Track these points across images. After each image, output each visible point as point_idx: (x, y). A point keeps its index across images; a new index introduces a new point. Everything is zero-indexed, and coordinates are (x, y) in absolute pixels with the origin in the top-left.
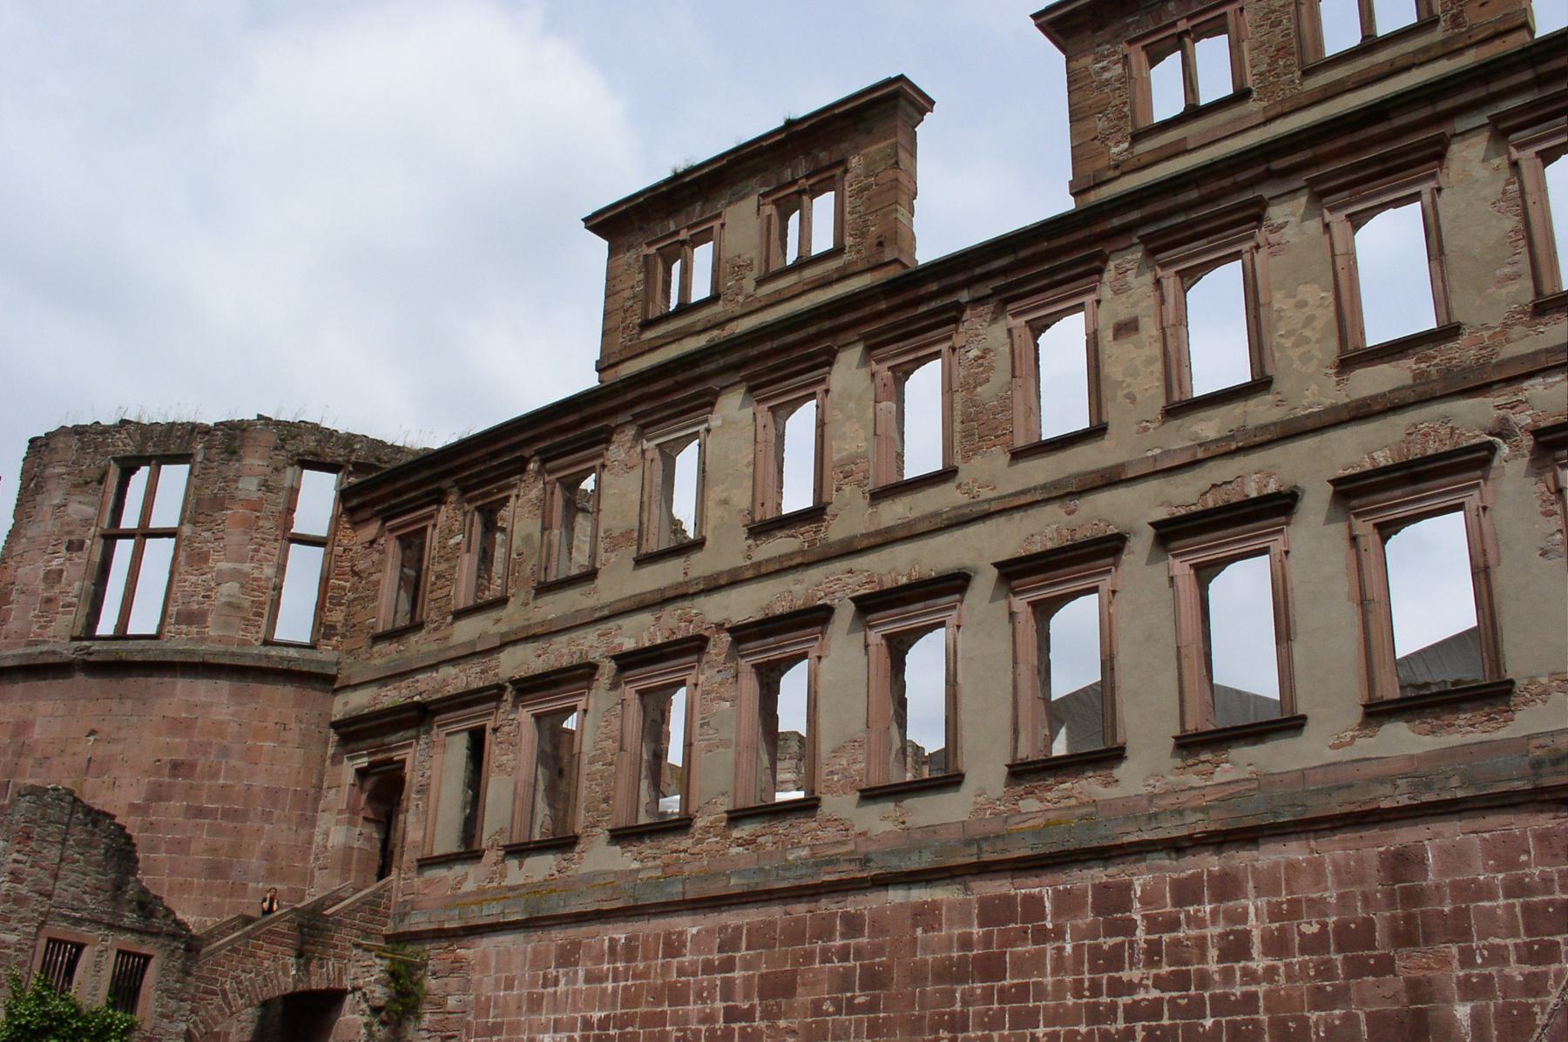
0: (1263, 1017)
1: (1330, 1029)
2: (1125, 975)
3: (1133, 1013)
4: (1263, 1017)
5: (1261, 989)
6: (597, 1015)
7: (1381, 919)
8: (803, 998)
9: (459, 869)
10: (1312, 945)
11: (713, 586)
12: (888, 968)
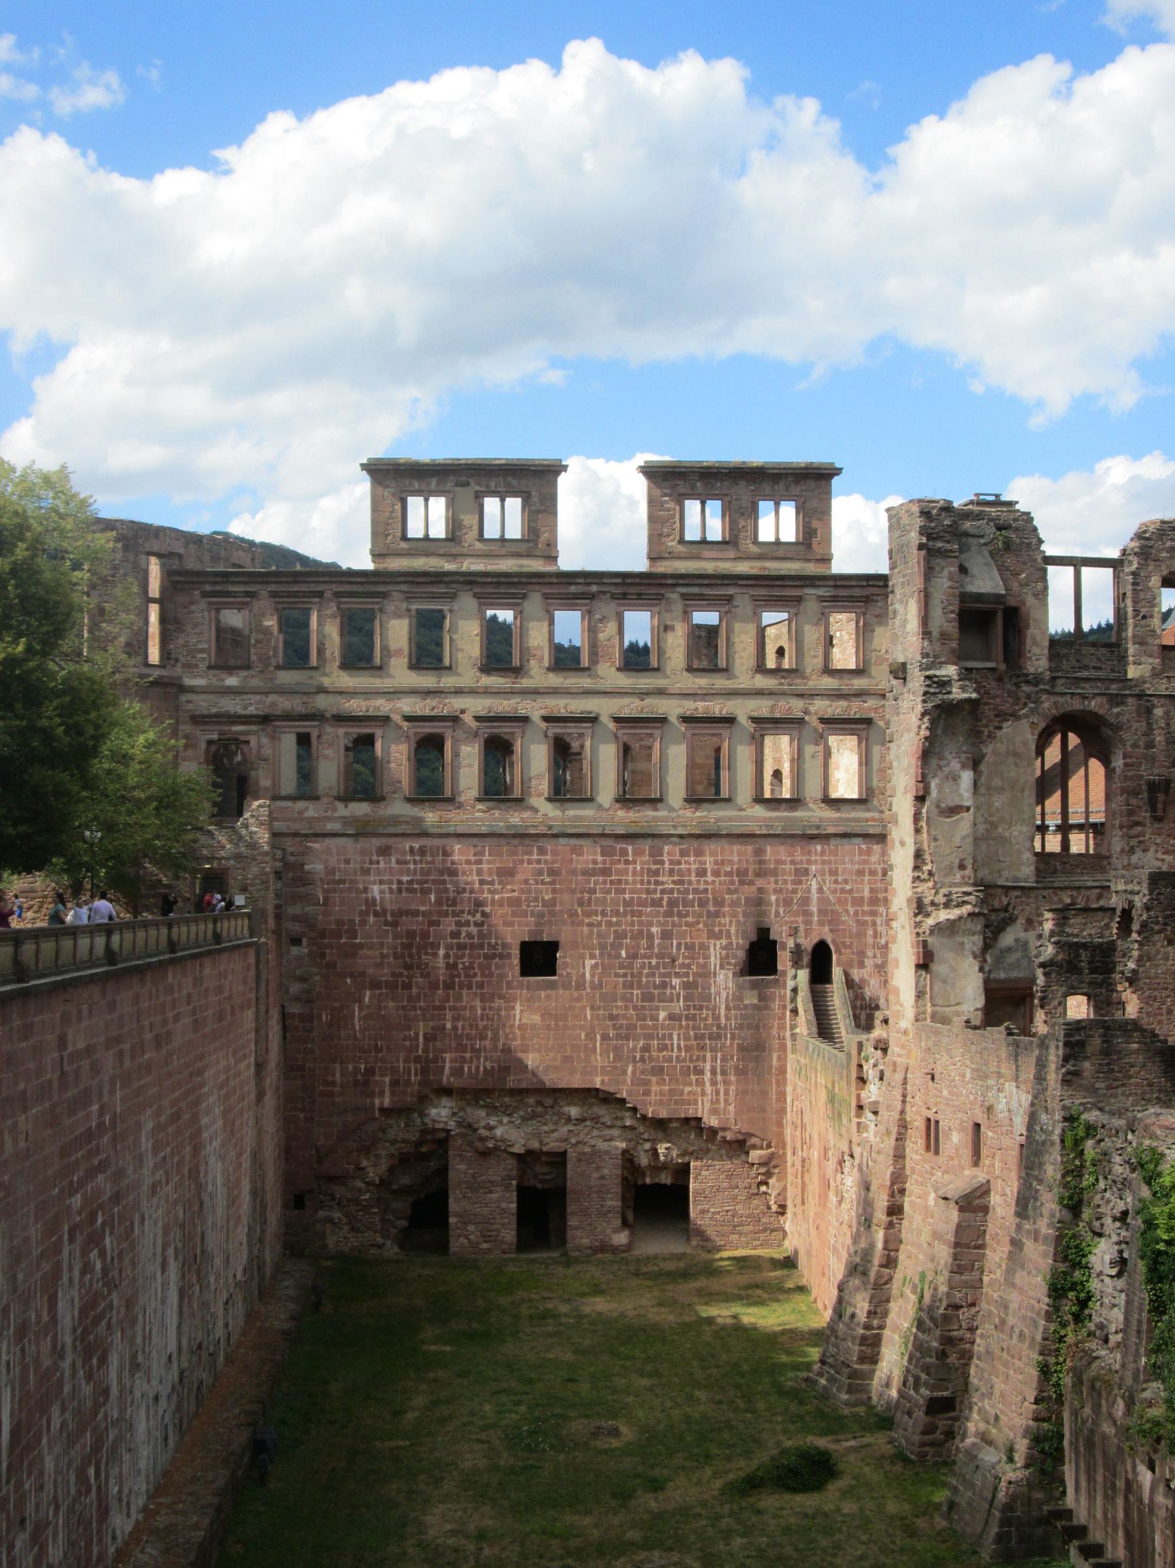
0: (710, 896)
1: (732, 901)
2: (660, 879)
3: (663, 892)
4: (710, 896)
5: (710, 887)
6: (405, 879)
7: (751, 867)
8: (519, 877)
9: (301, 804)
10: (727, 874)
11: (459, 692)
12: (560, 869)
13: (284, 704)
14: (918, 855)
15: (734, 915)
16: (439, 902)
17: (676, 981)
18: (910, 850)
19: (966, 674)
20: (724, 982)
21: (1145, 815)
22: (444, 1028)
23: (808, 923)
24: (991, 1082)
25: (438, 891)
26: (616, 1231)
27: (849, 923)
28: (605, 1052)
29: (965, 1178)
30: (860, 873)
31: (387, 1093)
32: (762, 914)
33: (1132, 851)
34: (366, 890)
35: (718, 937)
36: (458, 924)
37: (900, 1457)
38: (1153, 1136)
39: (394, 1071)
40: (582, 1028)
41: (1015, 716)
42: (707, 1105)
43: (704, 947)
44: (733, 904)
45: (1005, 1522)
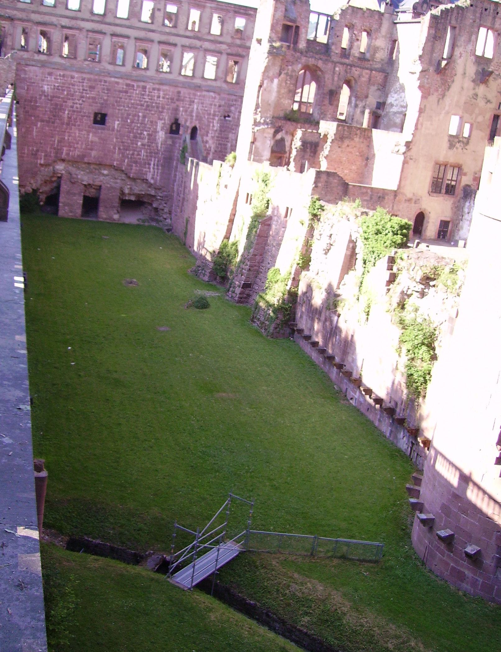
3: (145, 102)
6: (57, 85)
8: (96, 90)
10: (168, 99)
11: (83, 20)
13: (19, 15)
15: (168, 113)
16: (68, 94)
17: (145, 133)
20: (161, 135)
22: (64, 139)
23: (192, 119)
25: (68, 91)
26: (115, 214)
27: (205, 121)
28: (119, 154)
30: (211, 105)
31: (43, 159)
32: (178, 114)
34: (42, 87)
35: (161, 120)
36: (74, 103)
39: (46, 151)
40: (112, 145)
42: (151, 176)
43: (156, 123)
44: (168, 109)
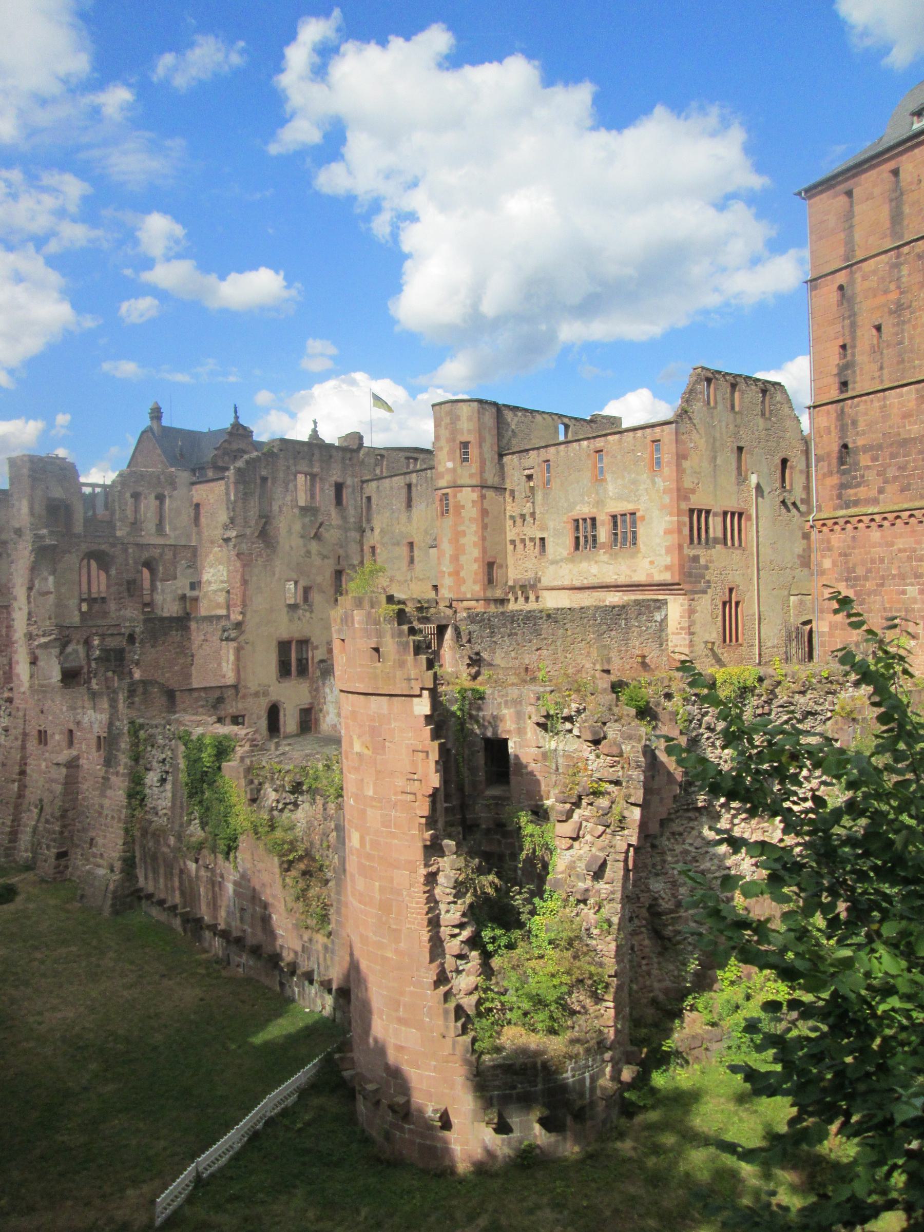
14: (29, 614)
18: (26, 611)
19: (52, 533)
21: (126, 594)
24: (79, 711)
29: (65, 755)
33: (120, 609)
37: (43, 880)
38: (184, 725)
41: (70, 552)
45: (114, 898)
